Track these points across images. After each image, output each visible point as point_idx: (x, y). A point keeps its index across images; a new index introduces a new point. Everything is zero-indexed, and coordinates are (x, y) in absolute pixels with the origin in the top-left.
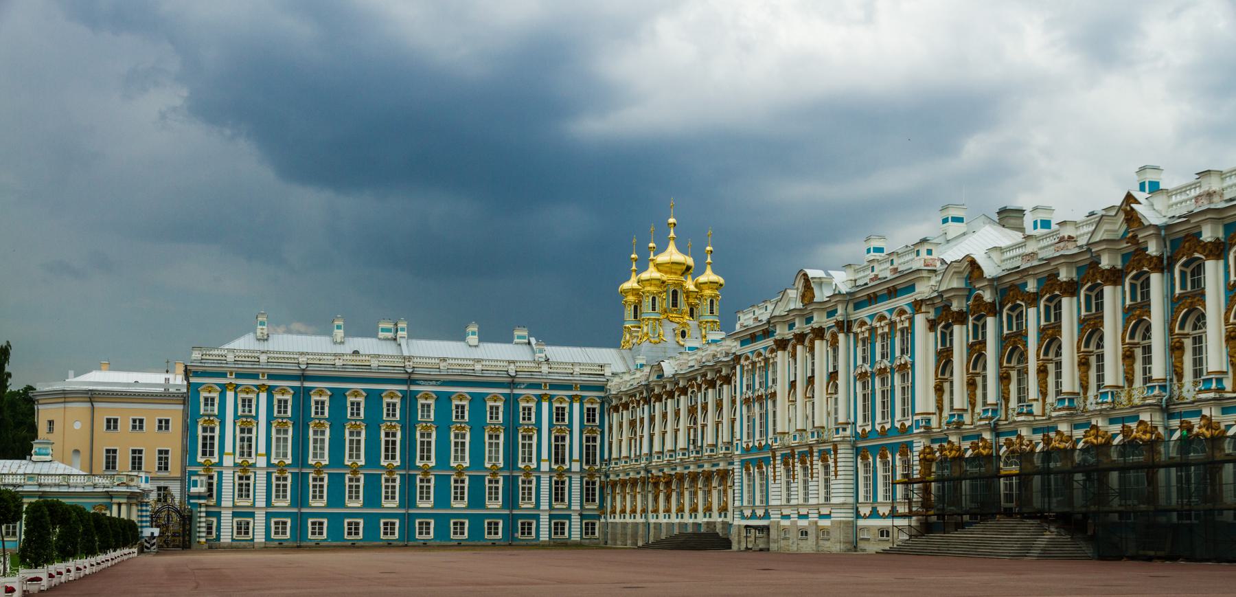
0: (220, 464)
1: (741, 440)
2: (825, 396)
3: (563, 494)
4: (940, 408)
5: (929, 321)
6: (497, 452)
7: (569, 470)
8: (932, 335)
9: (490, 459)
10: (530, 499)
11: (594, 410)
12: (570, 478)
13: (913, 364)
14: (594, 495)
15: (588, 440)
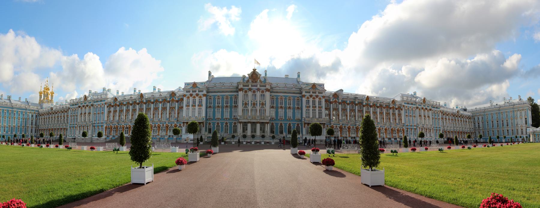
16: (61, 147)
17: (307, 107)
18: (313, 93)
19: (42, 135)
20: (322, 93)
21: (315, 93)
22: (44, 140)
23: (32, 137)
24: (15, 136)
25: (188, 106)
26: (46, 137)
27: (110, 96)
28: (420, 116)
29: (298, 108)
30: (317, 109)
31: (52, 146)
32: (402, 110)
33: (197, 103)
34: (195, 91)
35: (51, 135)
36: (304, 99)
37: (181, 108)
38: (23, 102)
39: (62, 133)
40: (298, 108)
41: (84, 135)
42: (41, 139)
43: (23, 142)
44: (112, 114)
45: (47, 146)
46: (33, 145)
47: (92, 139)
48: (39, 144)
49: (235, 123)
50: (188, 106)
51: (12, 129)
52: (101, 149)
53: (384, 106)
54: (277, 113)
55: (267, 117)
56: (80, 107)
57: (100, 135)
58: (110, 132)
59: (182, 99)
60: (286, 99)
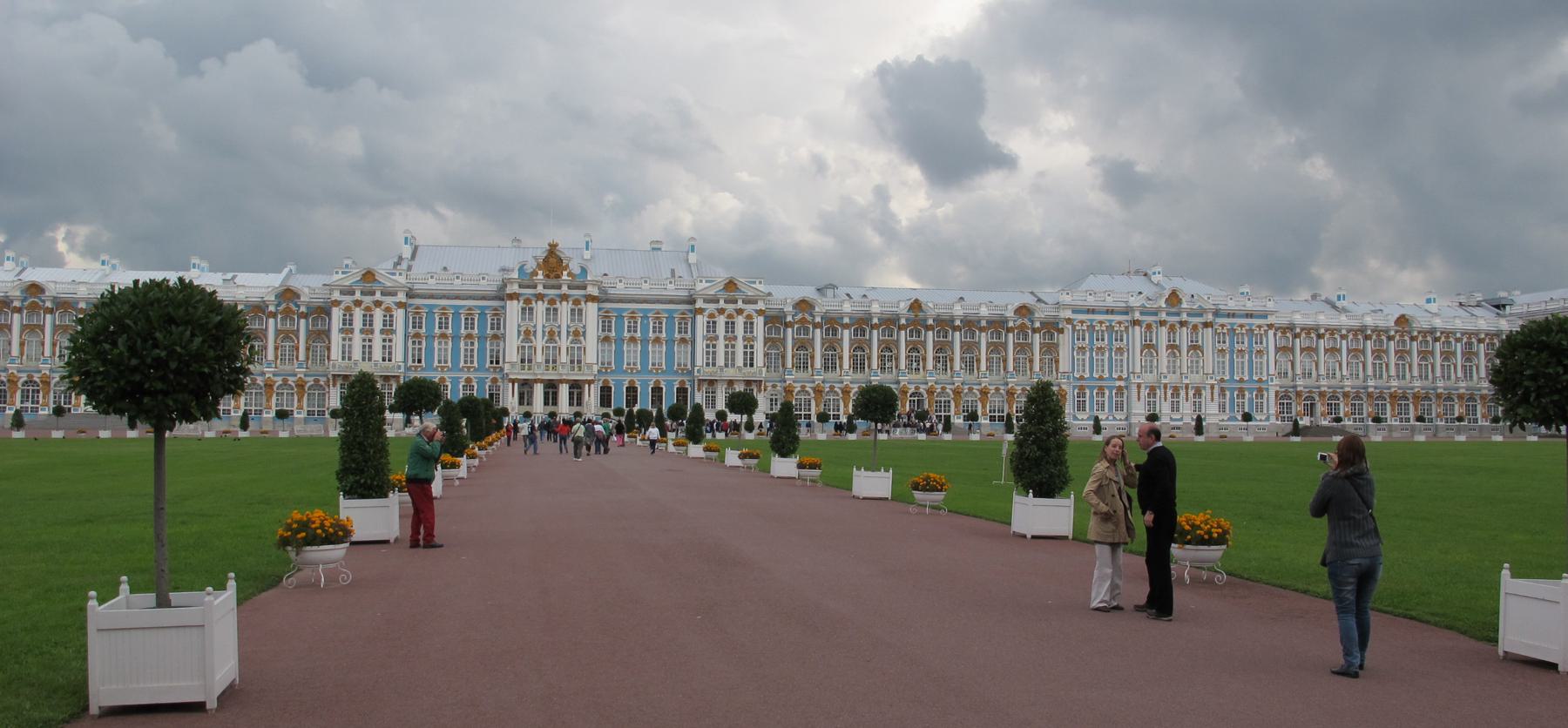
17: (710, 339)
18: (726, 302)
20: (755, 302)
21: (736, 302)
25: (347, 329)
28: (1149, 347)
29: (683, 340)
30: (740, 344)
32: (1061, 331)
33: (378, 324)
34: (373, 293)
36: (701, 321)
37: (320, 336)
40: (683, 340)
49: (494, 380)
50: (347, 329)
53: (983, 323)
54: (619, 354)
55: (590, 366)
59: (329, 314)
60: (645, 317)
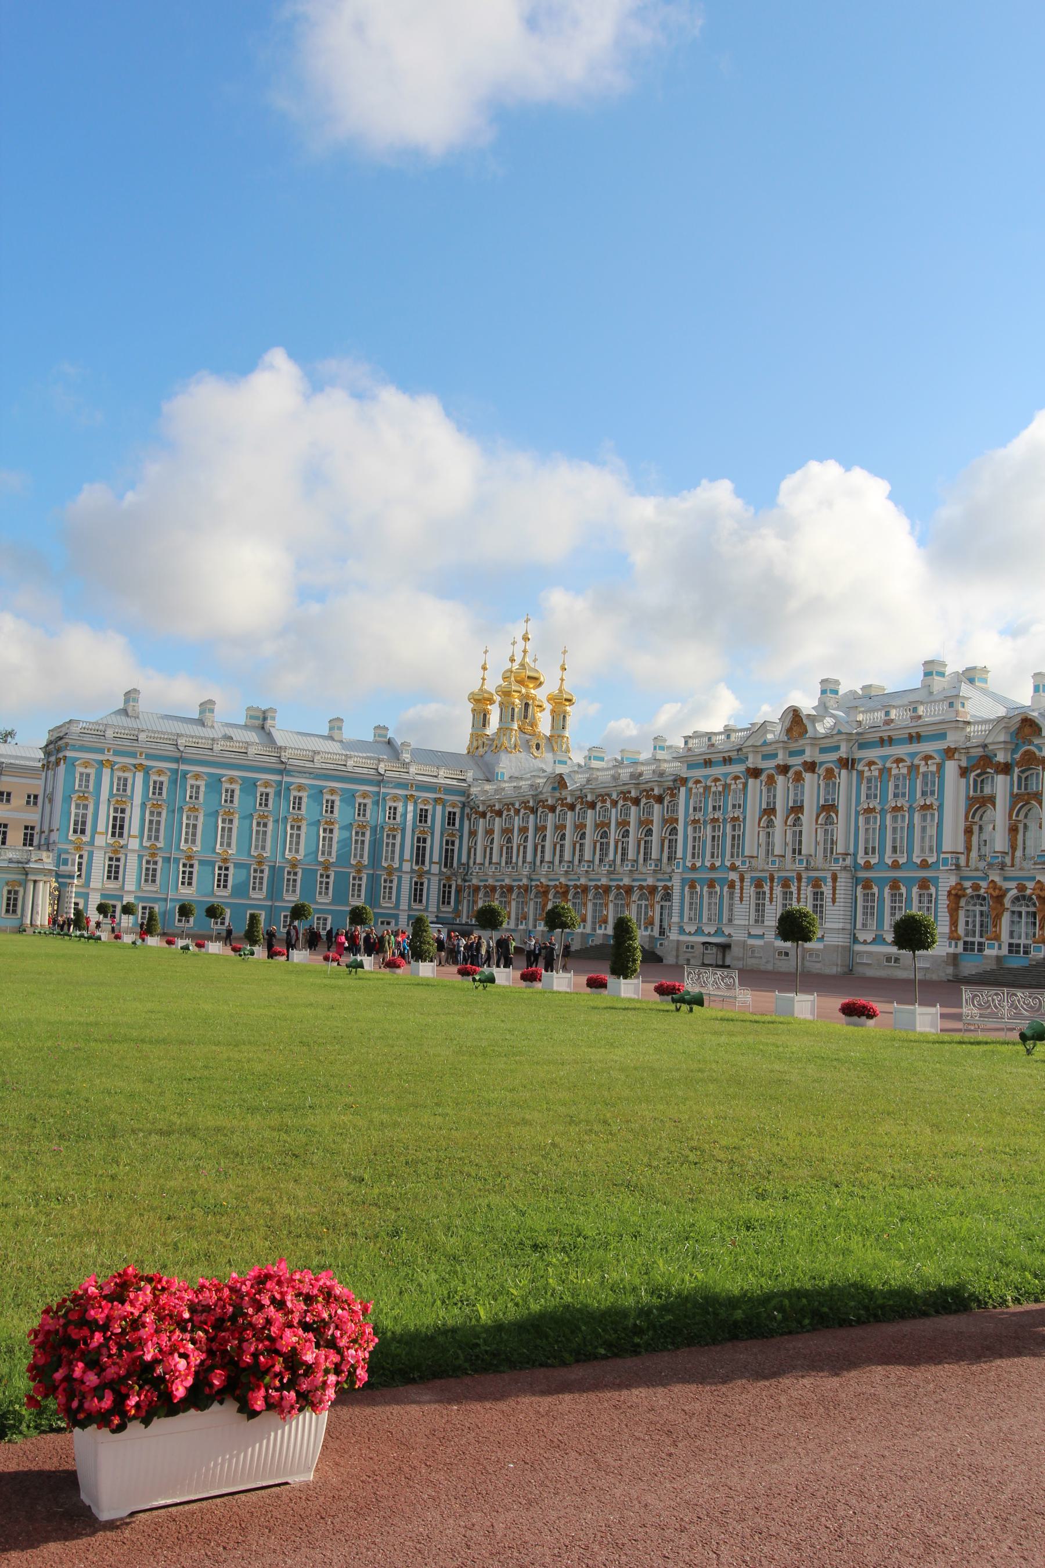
0: (92, 843)
1: (684, 858)
2: (814, 826)
3: (421, 895)
4: (969, 849)
5: (960, 767)
6: (362, 849)
7: (428, 872)
8: (963, 781)
9: (355, 856)
10: (390, 898)
11: (455, 814)
12: (429, 880)
13: (941, 807)
14: (449, 897)
15: (447, 844)
16: (629, 989)
19: (489, 919)
22: (503, 944)
23: (418, 924)
24: (298, 912)
26: (523, 925)
27: (980, 708)
31: (561, 981)
35: (555, 920)
38: (359, 745)
39: (631, 914)
41: (794, 927)
42: (487, 940)
43: (354, 948)
44: (999, 815)
45: (530, 977)
46: (426, 969)
47: (848, 951)
48: (469, 962)
51: (277, 879)
52: (926, 1019)
56: (755, 773)
57: (912, 934)
58: (989, 924)
